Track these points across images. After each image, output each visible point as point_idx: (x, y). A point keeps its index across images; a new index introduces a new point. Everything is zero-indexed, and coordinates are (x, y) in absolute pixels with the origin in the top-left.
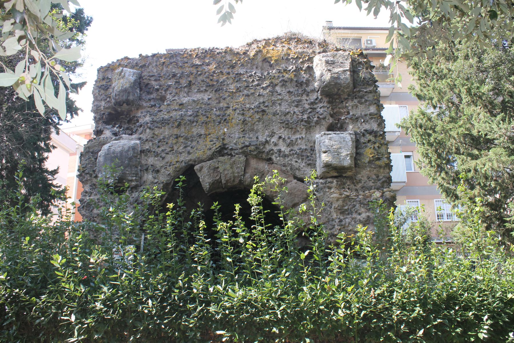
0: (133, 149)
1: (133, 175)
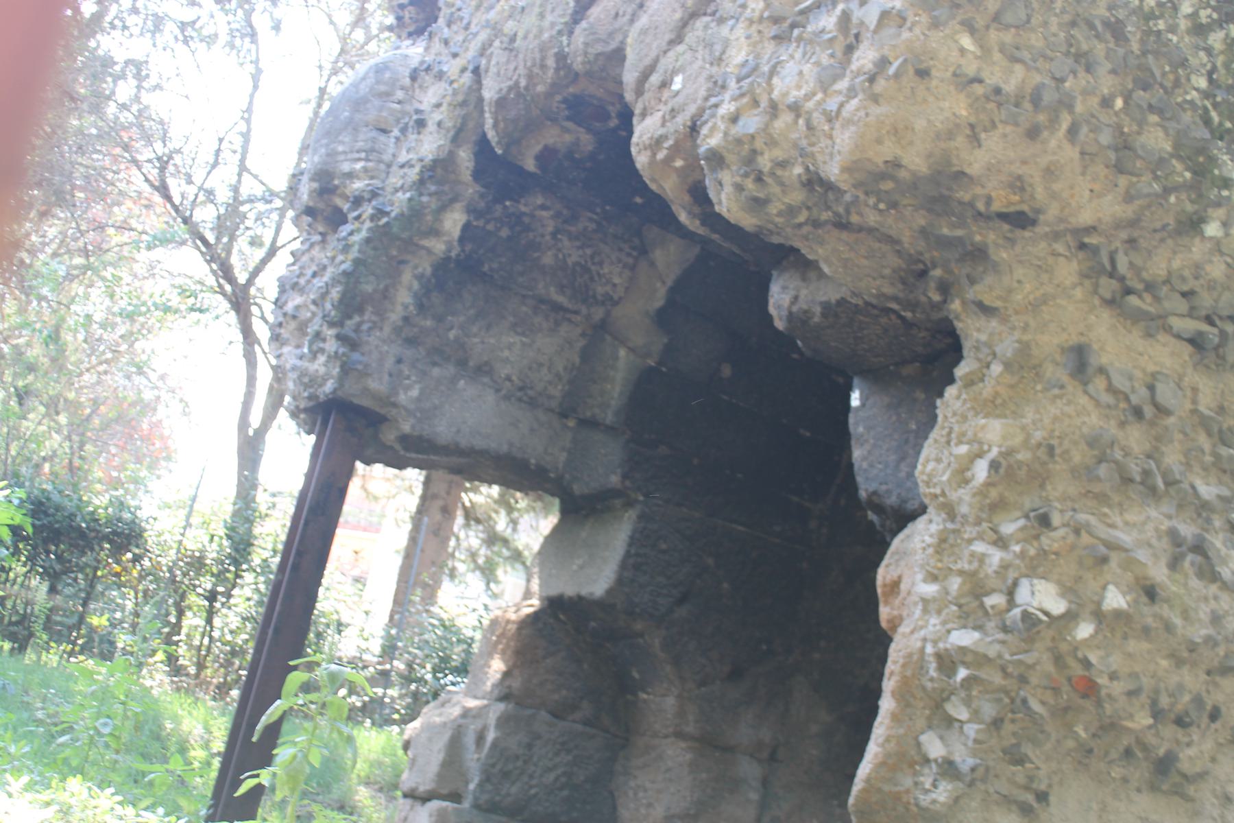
0: (377, 72)
1: (357, 156)
